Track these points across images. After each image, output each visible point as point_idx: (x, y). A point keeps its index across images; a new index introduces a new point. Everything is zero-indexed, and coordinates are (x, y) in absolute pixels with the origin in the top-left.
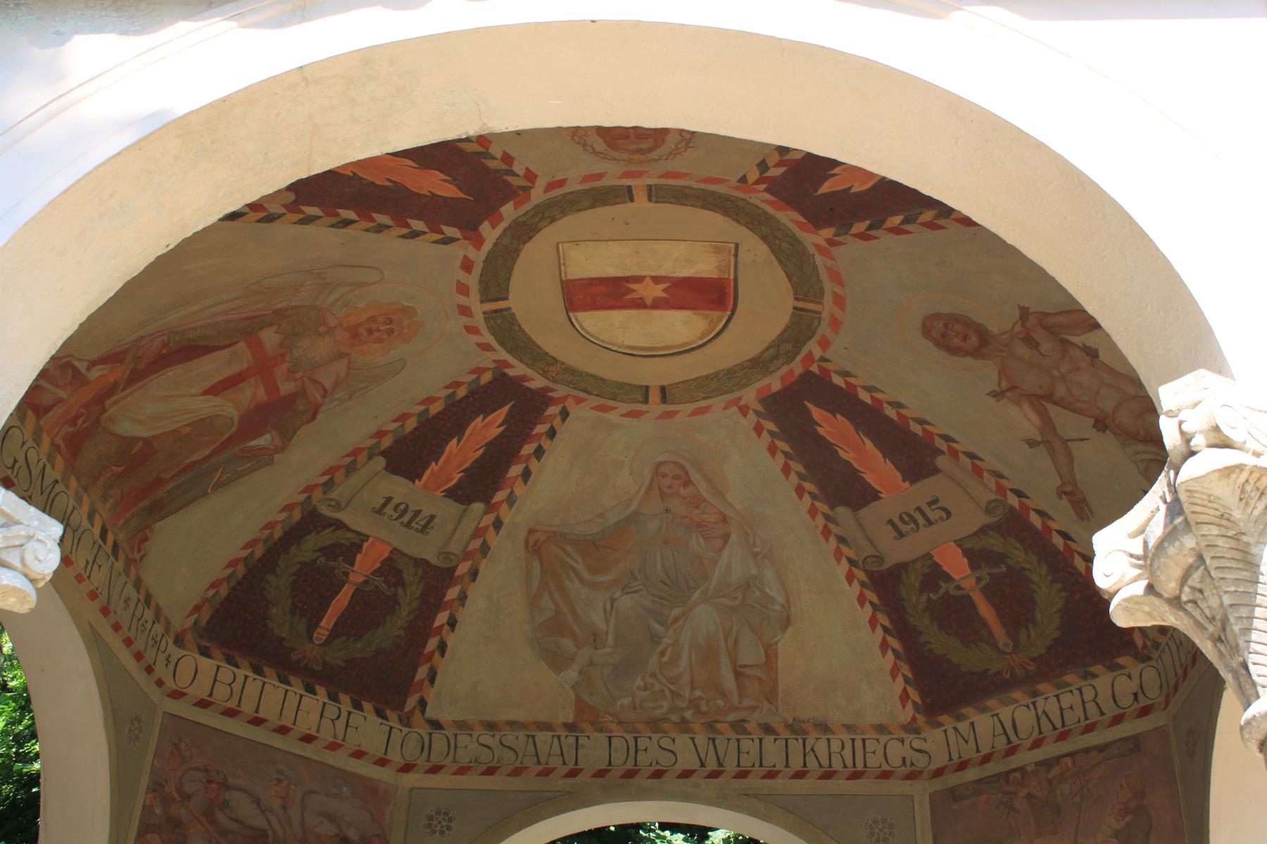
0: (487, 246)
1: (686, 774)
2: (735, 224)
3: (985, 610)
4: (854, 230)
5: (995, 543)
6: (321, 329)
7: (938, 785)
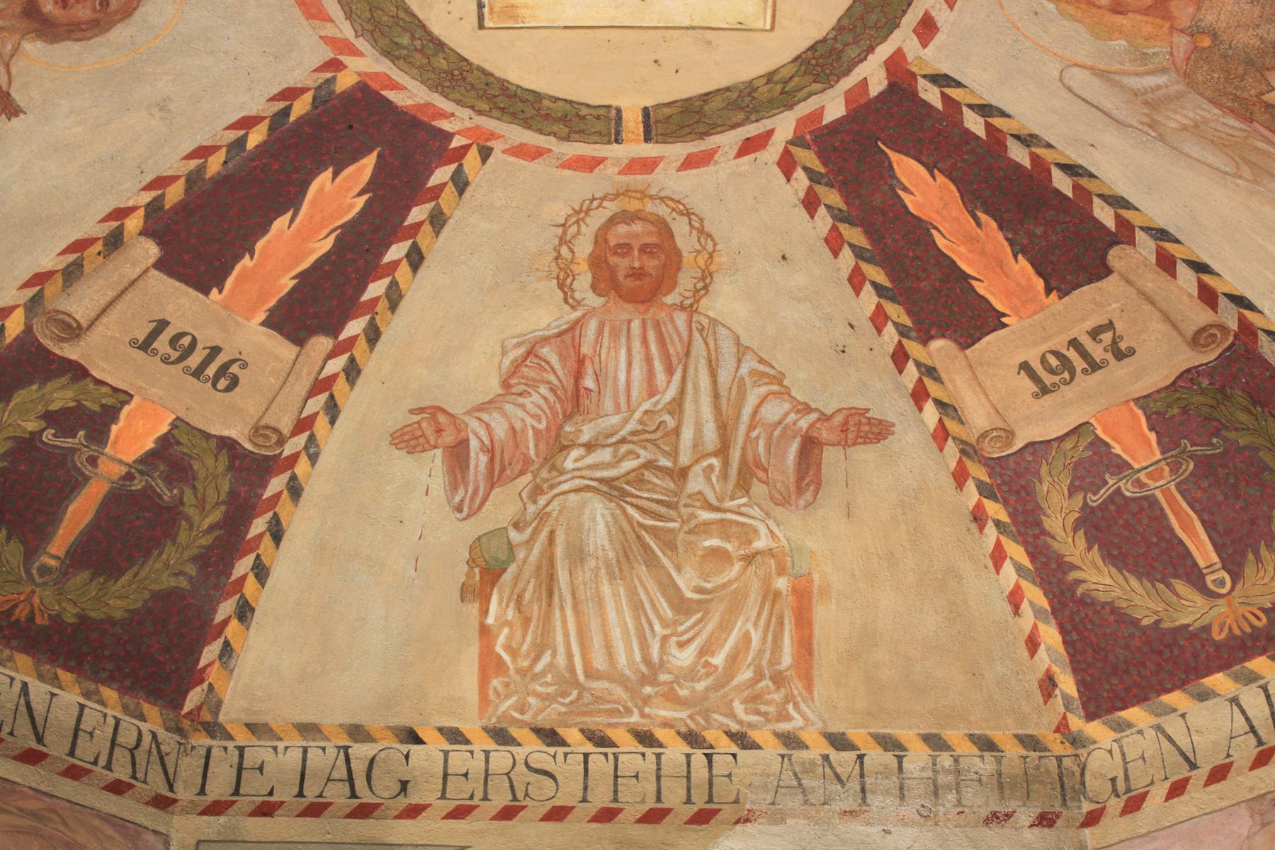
0: (884, 51)
2: (487, 66)
4: (308, 97)
6: (1206, 42)
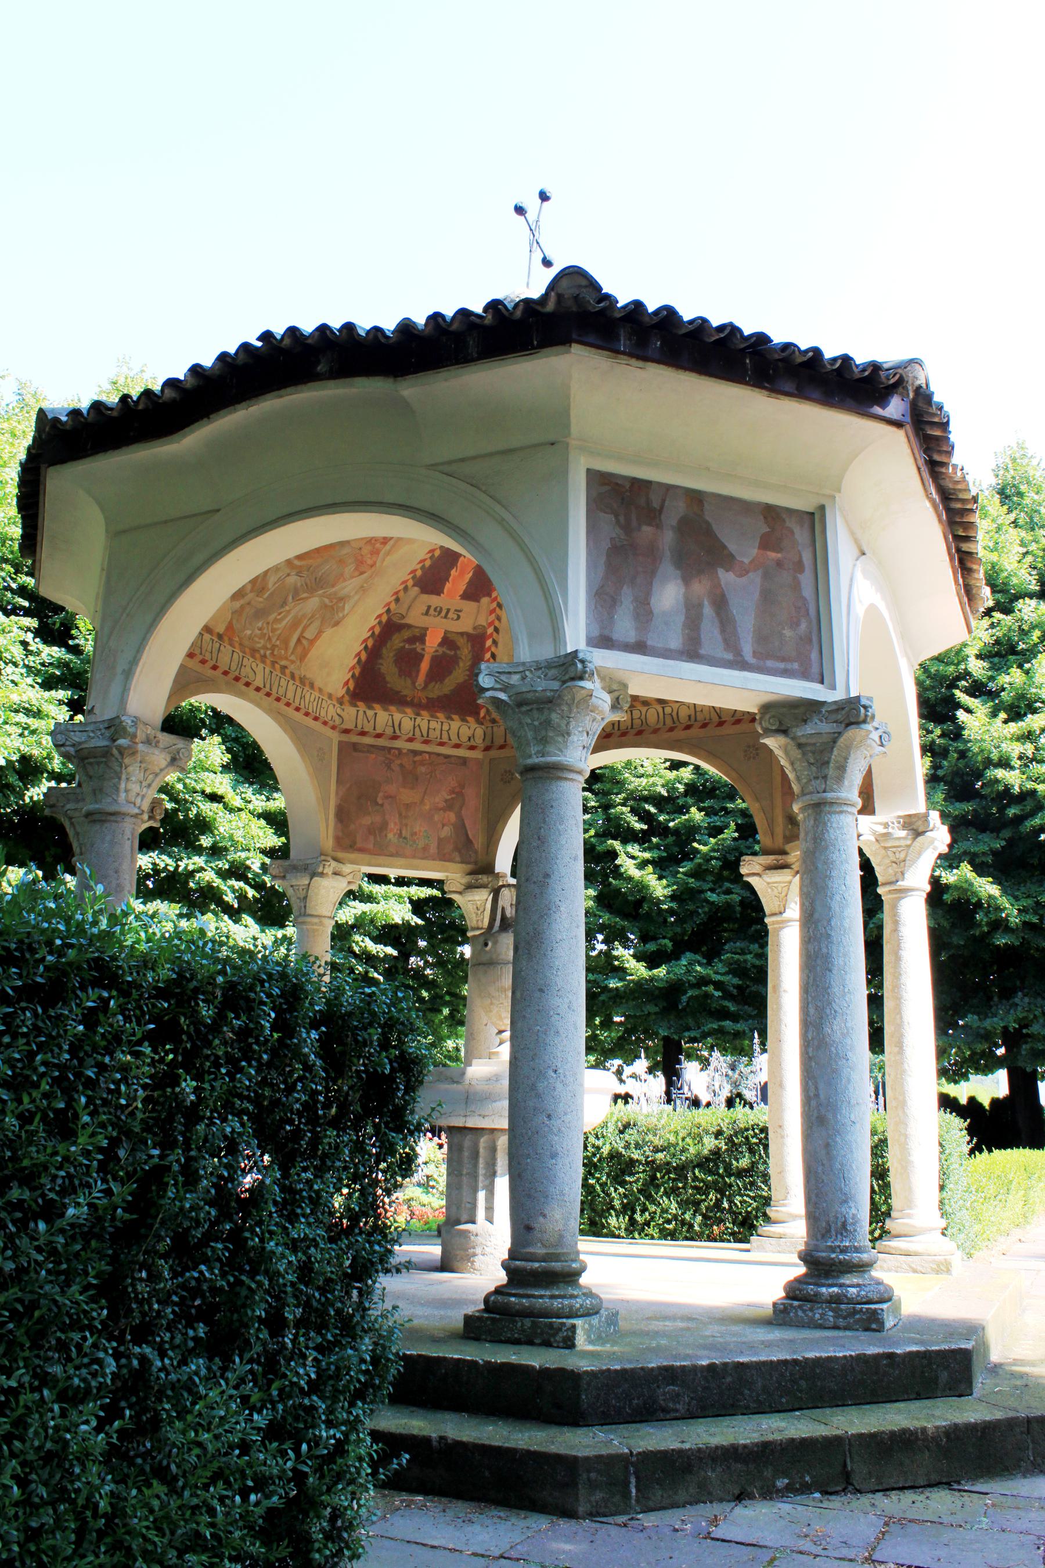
1: (258, 689)
3: (425, 666)
5: (461, 641)
7: (345, 738)
